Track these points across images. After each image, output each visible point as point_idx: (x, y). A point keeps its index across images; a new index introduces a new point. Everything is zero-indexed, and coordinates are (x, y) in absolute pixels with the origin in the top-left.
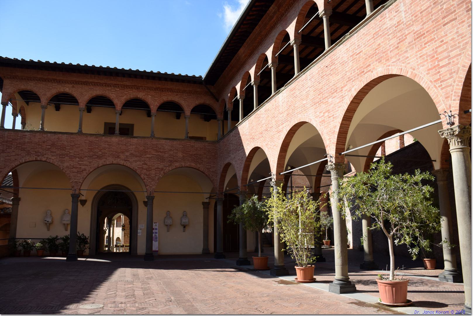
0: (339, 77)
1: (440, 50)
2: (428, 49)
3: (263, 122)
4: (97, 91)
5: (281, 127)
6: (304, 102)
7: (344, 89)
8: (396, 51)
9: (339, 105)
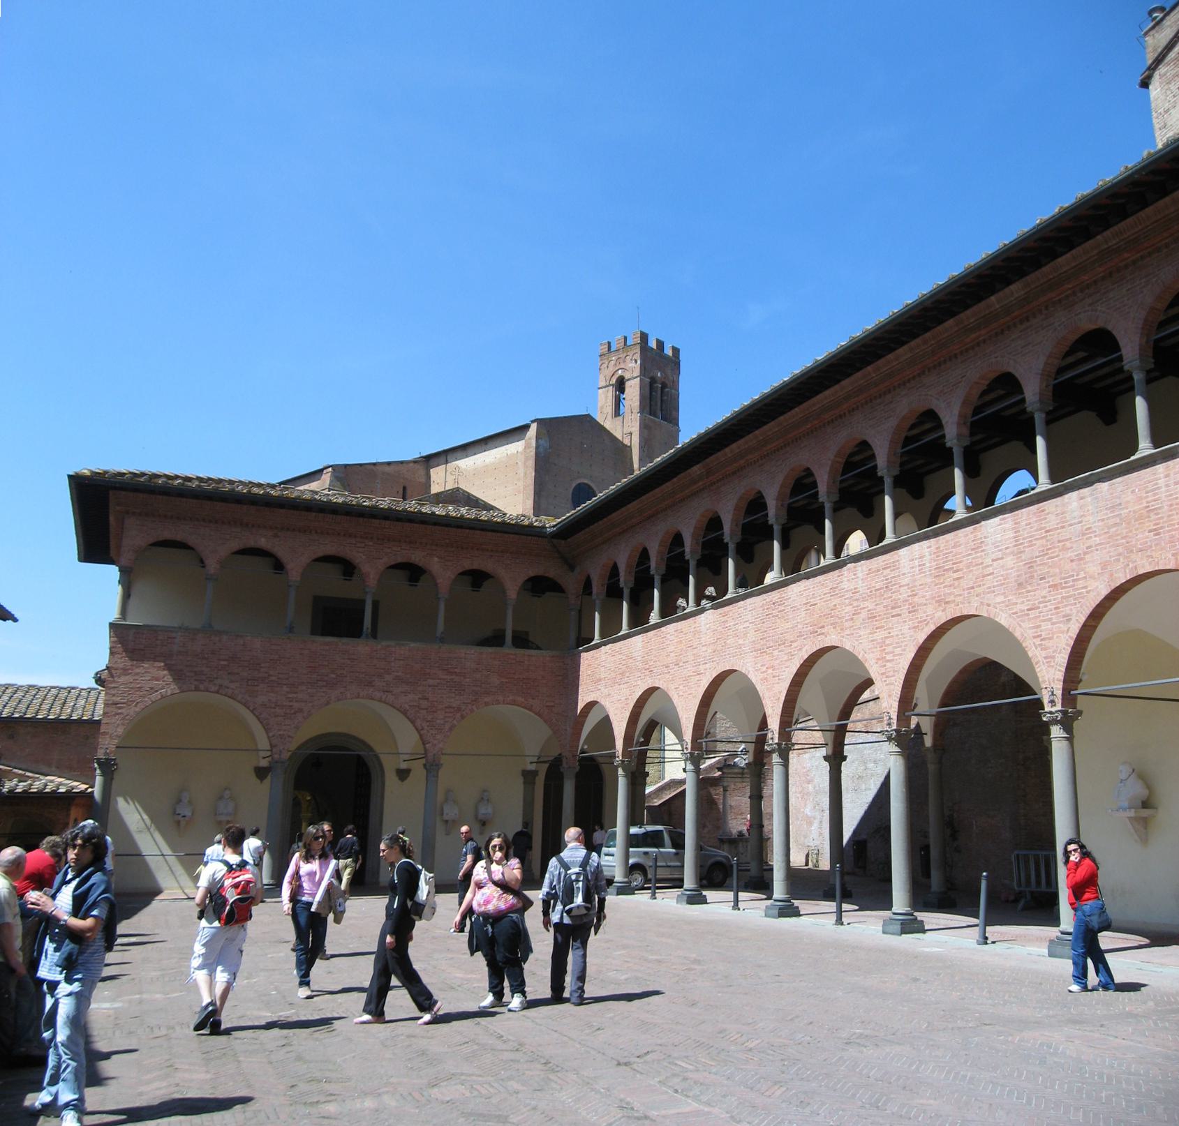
0: (789, 625)
1: (888, 642)
2: (879, 635)
3: (672, 648)
4: (329, 547)
5: (702, 667)
6: (741, 642)
7: (794, 645)
8: (850, 623)
9: (788, 664)
